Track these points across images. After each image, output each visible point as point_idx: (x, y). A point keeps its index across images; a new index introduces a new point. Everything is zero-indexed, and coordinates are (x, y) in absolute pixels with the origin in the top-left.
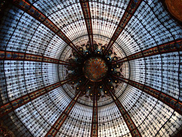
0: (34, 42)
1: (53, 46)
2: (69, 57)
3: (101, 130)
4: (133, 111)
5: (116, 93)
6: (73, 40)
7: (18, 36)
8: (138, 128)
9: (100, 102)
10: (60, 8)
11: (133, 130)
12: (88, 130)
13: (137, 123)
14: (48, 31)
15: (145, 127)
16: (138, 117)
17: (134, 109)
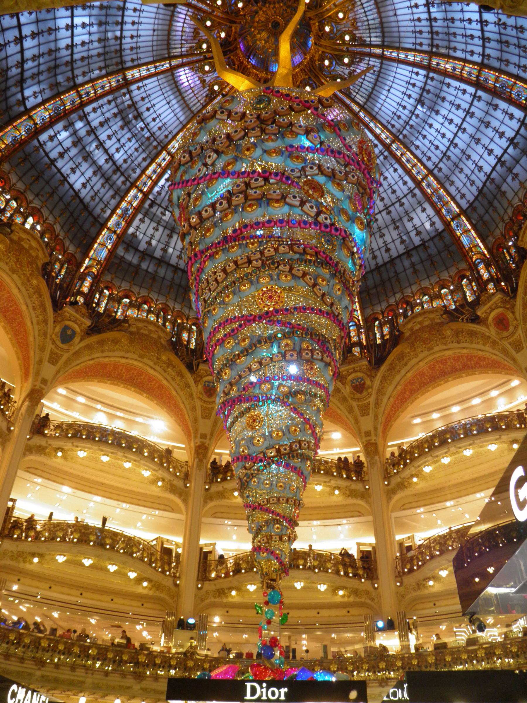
0: (118, 150)
1: (152, 110)
2: (204, 87)
3: (417, 143)
4: (440, 36)
5: (368, 39)
6: (166, 52)
7: (85, 181)
8: (486, 61)
9: (357, 93)
10: (69, 41)
11: (478, 77)
12: (391, 170)
13: (472, 53)
14: (109, 102)
15: (498, 46)
16: (464, 40)
17: (440, 30)
